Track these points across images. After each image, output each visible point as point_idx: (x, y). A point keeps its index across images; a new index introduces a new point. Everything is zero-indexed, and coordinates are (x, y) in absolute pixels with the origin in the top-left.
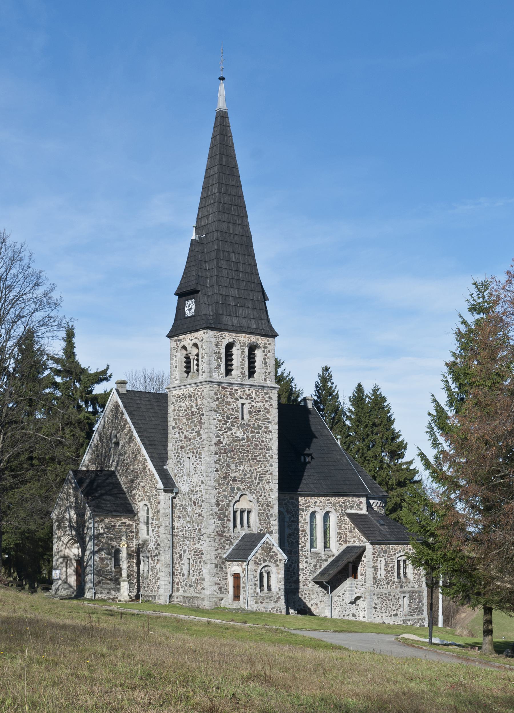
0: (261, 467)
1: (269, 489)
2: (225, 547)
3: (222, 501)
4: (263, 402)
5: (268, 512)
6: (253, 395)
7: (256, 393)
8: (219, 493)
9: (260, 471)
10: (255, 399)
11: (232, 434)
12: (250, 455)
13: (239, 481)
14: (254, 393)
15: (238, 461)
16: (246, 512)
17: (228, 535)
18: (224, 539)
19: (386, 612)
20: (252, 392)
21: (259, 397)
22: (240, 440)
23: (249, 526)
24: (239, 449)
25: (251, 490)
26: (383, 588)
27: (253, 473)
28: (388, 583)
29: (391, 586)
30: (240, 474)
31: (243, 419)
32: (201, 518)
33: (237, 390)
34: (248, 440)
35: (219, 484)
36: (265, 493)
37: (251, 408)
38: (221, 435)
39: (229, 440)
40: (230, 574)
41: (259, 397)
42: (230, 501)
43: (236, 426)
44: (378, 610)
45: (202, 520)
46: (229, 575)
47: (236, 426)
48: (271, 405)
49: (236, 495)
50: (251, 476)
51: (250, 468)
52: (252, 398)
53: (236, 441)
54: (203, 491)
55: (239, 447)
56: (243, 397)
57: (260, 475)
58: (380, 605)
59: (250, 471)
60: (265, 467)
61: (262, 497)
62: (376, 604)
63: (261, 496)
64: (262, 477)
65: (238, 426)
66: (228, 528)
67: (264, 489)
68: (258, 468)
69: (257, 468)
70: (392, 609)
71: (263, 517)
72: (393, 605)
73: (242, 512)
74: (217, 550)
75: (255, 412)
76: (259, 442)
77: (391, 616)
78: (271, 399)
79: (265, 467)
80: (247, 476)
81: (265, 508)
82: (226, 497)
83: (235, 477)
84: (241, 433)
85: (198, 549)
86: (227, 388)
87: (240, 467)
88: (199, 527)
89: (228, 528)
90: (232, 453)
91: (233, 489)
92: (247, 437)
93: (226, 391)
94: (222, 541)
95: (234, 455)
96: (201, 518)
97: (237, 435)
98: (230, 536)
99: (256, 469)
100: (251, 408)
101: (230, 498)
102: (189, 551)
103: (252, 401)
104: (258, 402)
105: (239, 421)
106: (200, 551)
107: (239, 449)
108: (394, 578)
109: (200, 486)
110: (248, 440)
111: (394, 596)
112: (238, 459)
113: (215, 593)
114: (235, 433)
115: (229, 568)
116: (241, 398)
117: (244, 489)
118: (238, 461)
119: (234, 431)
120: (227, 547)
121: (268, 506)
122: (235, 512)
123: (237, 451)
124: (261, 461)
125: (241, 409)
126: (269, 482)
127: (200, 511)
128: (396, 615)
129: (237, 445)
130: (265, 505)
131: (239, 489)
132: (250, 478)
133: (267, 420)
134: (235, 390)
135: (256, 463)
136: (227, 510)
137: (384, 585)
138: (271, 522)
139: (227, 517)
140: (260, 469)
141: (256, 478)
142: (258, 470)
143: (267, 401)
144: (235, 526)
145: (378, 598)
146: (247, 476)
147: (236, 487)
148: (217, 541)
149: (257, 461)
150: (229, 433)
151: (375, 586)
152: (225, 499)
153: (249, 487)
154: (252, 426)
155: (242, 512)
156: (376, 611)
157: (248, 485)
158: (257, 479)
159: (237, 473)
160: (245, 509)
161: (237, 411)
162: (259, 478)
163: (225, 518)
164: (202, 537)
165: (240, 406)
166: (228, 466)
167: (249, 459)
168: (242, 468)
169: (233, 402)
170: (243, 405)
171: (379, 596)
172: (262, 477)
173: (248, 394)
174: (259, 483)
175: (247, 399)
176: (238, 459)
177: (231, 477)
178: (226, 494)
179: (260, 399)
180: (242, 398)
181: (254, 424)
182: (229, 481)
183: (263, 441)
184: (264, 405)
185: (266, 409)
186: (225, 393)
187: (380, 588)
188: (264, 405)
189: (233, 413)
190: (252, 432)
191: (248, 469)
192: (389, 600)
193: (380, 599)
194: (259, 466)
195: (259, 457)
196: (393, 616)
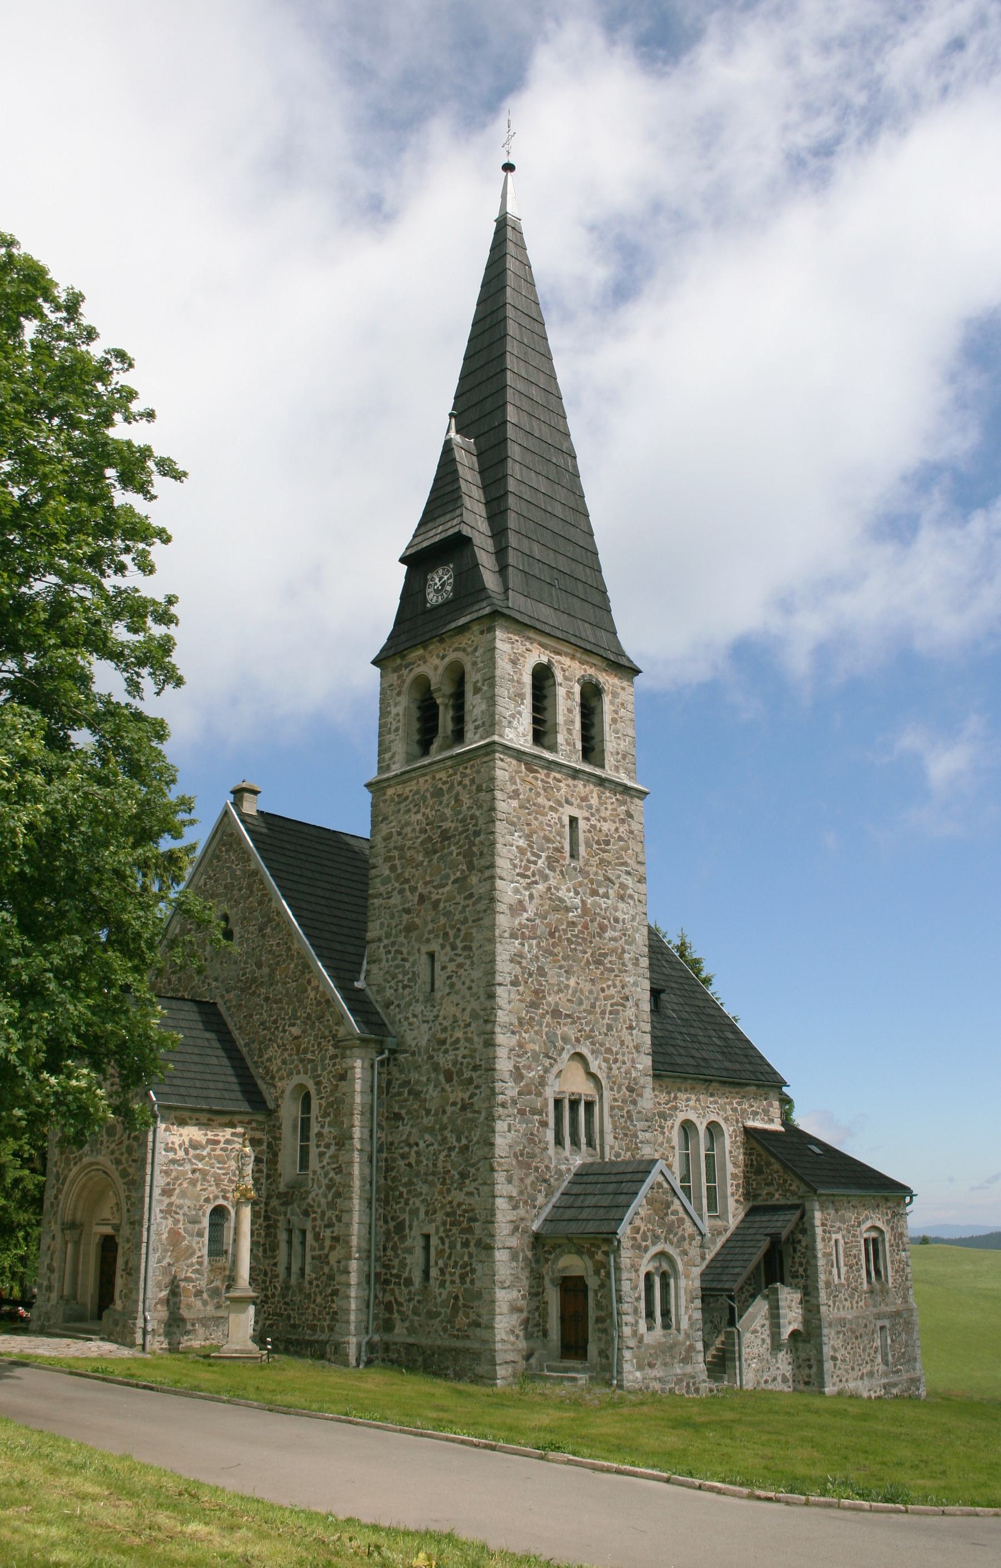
0: (615, 986)
1: (631, 1045)
2: (534, 1199)
3: (529, 1068)
4: (614, 822)
5: (632, 1107)
6: (594, 801)
7: (600, 797)
8: (521, 1045)
9: (612, 997)
10: (598, 810)
11: (549, 889)
12: (590, 951)
13: (567, 1016)
14: (595, 795)
15: (563, 962)
16: (583, 1103)
17: (542, 1167)
18: (532, 1178)
19: (853, 1369)
20: (592, 792)
21: (606, 809)
22: (568, 910)
23: (590, 1143)
24: (565, 931)
25: (593, 1043)
26: (844, 1307)
27: (597, 999)
28: (852, 1296)
29: (857, 1302)
30: (569, 997)
31: (573, 856)
32: (470, 1115)
33: (560, 781)
34: (585, 911)
35: (521, 1021)
36: (624, 1055)
37: (590, 831)
38: (526, 889)
39: (542, 905)
40: (552, 1281)
41: (606, 809)
42: (546, 1071)
43: (558, 870)
44: (839, 1362)
45: (473, 1120)
46: (547, 1282)
47: (558, 870)
48: (631, 832)
49: (560, 1055)
50: (593, 1006)
51: (588, 986)
52: (590, 807)
53: (556, 909)
54: (476, 1039)
55: (564, 927)
56: (573, 800)
57: (612, 1005)
58: (843, 1351)
59: (591, 992)
60: (623, 987)
61: (618, 1064)
62: (835, 1350)
63: (616, 1061)
64: (617, 1012)
65: (561, 872)
66: (542, 1145)
67: (622, 1043)
68: (609, 987)
69: (604, 986)
70: (863, 1360)
71: (622, 1120)
72: (864, 1350)
73: (574, 1104)
74: (515, 1207)
75: (598, 843)
76: (609, 921)
77: (862, 1378)
78: (631, 816)
79: (623, 987)
80: (584, 1007)
81: (624, 1095)
82: (535, 1056)
83: (557, 1004)
84: (569, 890)
85: (459, 1205)
86: (537, 772)
87: (568, 979)
88: (464, 1141)
89: (542, 1145)
90: (551, 941)
91: (551, 1039)
92: (583, 901)
93: (537, 779)
94: (528, 1181)
95: (554, 945)
96: (470, 1115)
97: (560, 894)
98: (547, 1167)
99: (603, 990)
100: (590, 831)
101: (547, 1062)
102: (427, 1213)
103: (592, 815)
104: (605, 820)
105: (564, 858)
106: (465, 1211)
107: (565, 931)
108: (861, 1284)
109: (469, 1025)
110: (585, 911)
111: (866, 1326)
112: (564, 959)
113: (512, 1338)
114: (557, 889)
115: (547, 1260)
116: (567, 802)
117: (578, 1040)
118: (563, 962)
119: (552, 882)
120: (540, 1199)
121: (631, 1090)
122: (558, 1103)
123: (560, 937)
124: (612, 970)
125: (567, 828)
126: (631, 1028)
127: (466, 1096)
128: (871, 1374)
129: (560, 921)
130: (624, 1088)
131: (565, 1039)
132: (589, 1013)
133: (624, 868)
134: (555, 778)
135: (602, 973)
136: (539, 1094)
137: (846, 1300)
138: (639, 1133)
139: (540, 1113)
140: (612, 991)
141: (603, 1013)
142: (607, 992)
143: (623, 821)
144: (559, 1141)
145: (838, 1332)
146: (584, 1007)
147: (559, 1032)
148: (516, 1181)
149: (607, 969)
150: (541, 887)
151: (831, 1303)
152: (534, 1065)
153: (588, 1037)
154: (592, 876)
155: (574, 1104)
156: (835, 1365)
157: (587, 1029)
158: (607, 1015)
159: (561, 995)
160: (580, 1095)
161: (560, 834)
162: (611, 1013)
163: (536, 1117)
164: (473, 1170)
165: (566, 821)
166: (541, 972)
167: (588, 963)
168: (572, 982)
169: (552, 808)
170: (573, 820)
171: (839, 1328)
172: (617, 1012)
173: (583, 795)
174: (609, 1027)
175: (580, 807)
176: (564, 959)
177: (549, 1004)
178: (537, 1048)
179: (609, 812)
180: (571, 804)
181: (596, 874)
182: (543, 1016)
183: (616, 920)
184: (617, 830)
185: (620, 839)
186: (533, 781)
187: (838, 1309)
188: (617, 830)
189: (551, 836)
190: (594, 893)
191: (587, 987)
192: (857, 1338)
193: (841, 1336)
194: (610, 983)
195: (609, 958)
196: (865, 1378)
